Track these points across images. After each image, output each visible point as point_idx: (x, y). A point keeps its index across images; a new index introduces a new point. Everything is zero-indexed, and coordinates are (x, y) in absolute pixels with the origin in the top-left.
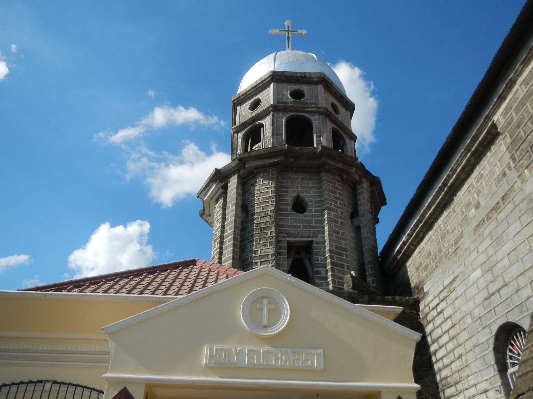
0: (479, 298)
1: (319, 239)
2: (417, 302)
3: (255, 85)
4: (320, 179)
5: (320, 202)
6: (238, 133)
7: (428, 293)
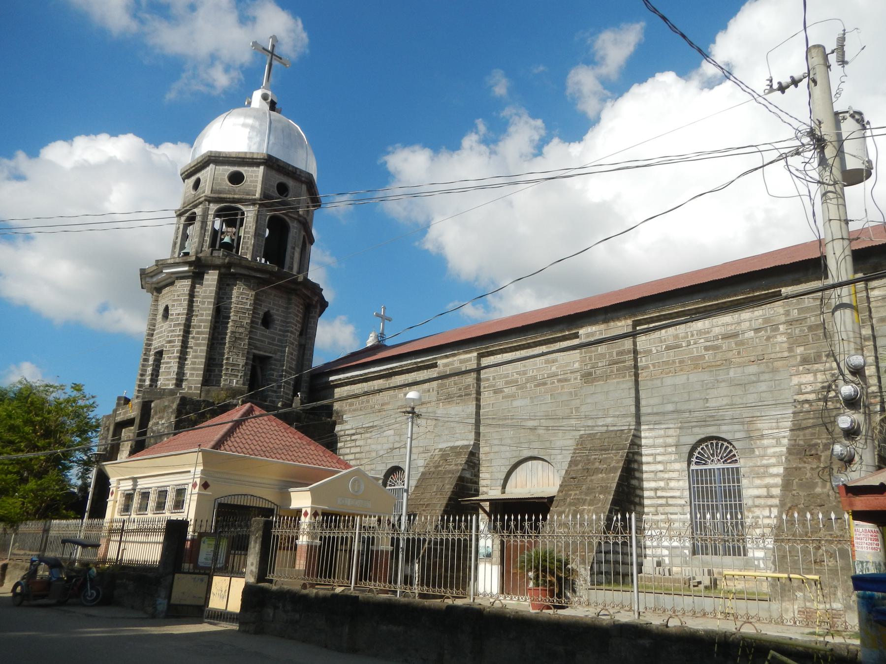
0: (386, 446)
1: (278, 357)
2: (334, 424)
3: (243, 156)
4: (289, 299)
5: (284, 322)
6: (210, 202)
7: (346, 422)
